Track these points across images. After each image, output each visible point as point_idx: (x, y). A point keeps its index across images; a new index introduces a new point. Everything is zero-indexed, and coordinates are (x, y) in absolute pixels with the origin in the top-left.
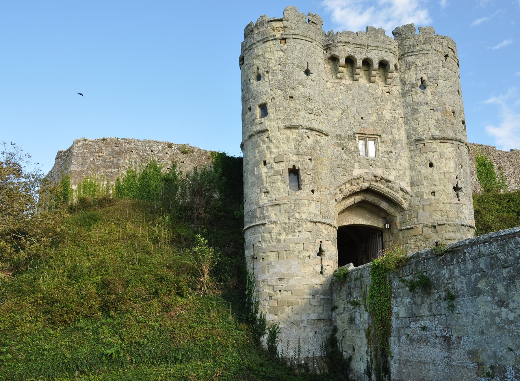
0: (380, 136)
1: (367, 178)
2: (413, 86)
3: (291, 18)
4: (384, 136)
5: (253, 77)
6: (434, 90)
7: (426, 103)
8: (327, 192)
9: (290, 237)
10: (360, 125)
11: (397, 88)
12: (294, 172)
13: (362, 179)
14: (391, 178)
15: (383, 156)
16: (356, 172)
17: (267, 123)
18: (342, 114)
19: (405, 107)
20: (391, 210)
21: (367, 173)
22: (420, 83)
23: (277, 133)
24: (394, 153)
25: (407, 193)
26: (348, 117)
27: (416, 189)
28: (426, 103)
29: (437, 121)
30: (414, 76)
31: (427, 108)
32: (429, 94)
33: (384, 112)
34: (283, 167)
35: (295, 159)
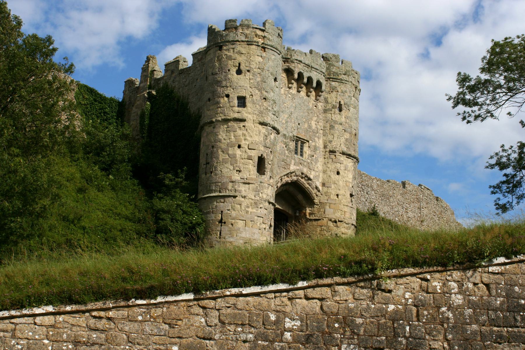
0: (308, 141)
1: (297, 174)
2: (334, 107)
7: (341, 124)
9: (254, 210)
12: (261, 161)
13: (294, 174)
14: (312, 177)
16: (293, 168)
17: (244, 113)
18: (288, 118)
19: (325, 122)
21: (298, 169)
23: (252, 125)
24: (314, 157)
25: (319, 191)
27: (325, 189)
29: (346, 140)
30: (335, 99)
31: (341, 128)
32: (343, 117)
34: (255, 155)
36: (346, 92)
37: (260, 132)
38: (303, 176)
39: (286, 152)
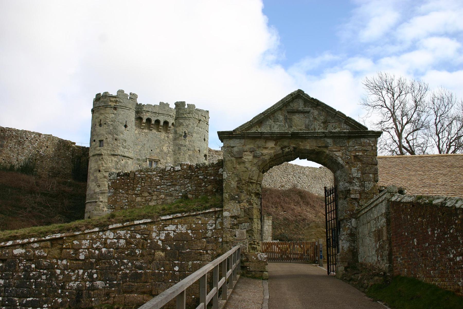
2: (181, 136)
3: (121, 96)
4: (162, 160)
5: (98, 124)
6: (190, 139)
7: (185, 146)
11: (172, 135)
22: (183, 135)
26: (144, 150)
28: (185, 146)
29: (189, 155)
33: (164, 148)
36: (189, 124)
37: (112, 160)
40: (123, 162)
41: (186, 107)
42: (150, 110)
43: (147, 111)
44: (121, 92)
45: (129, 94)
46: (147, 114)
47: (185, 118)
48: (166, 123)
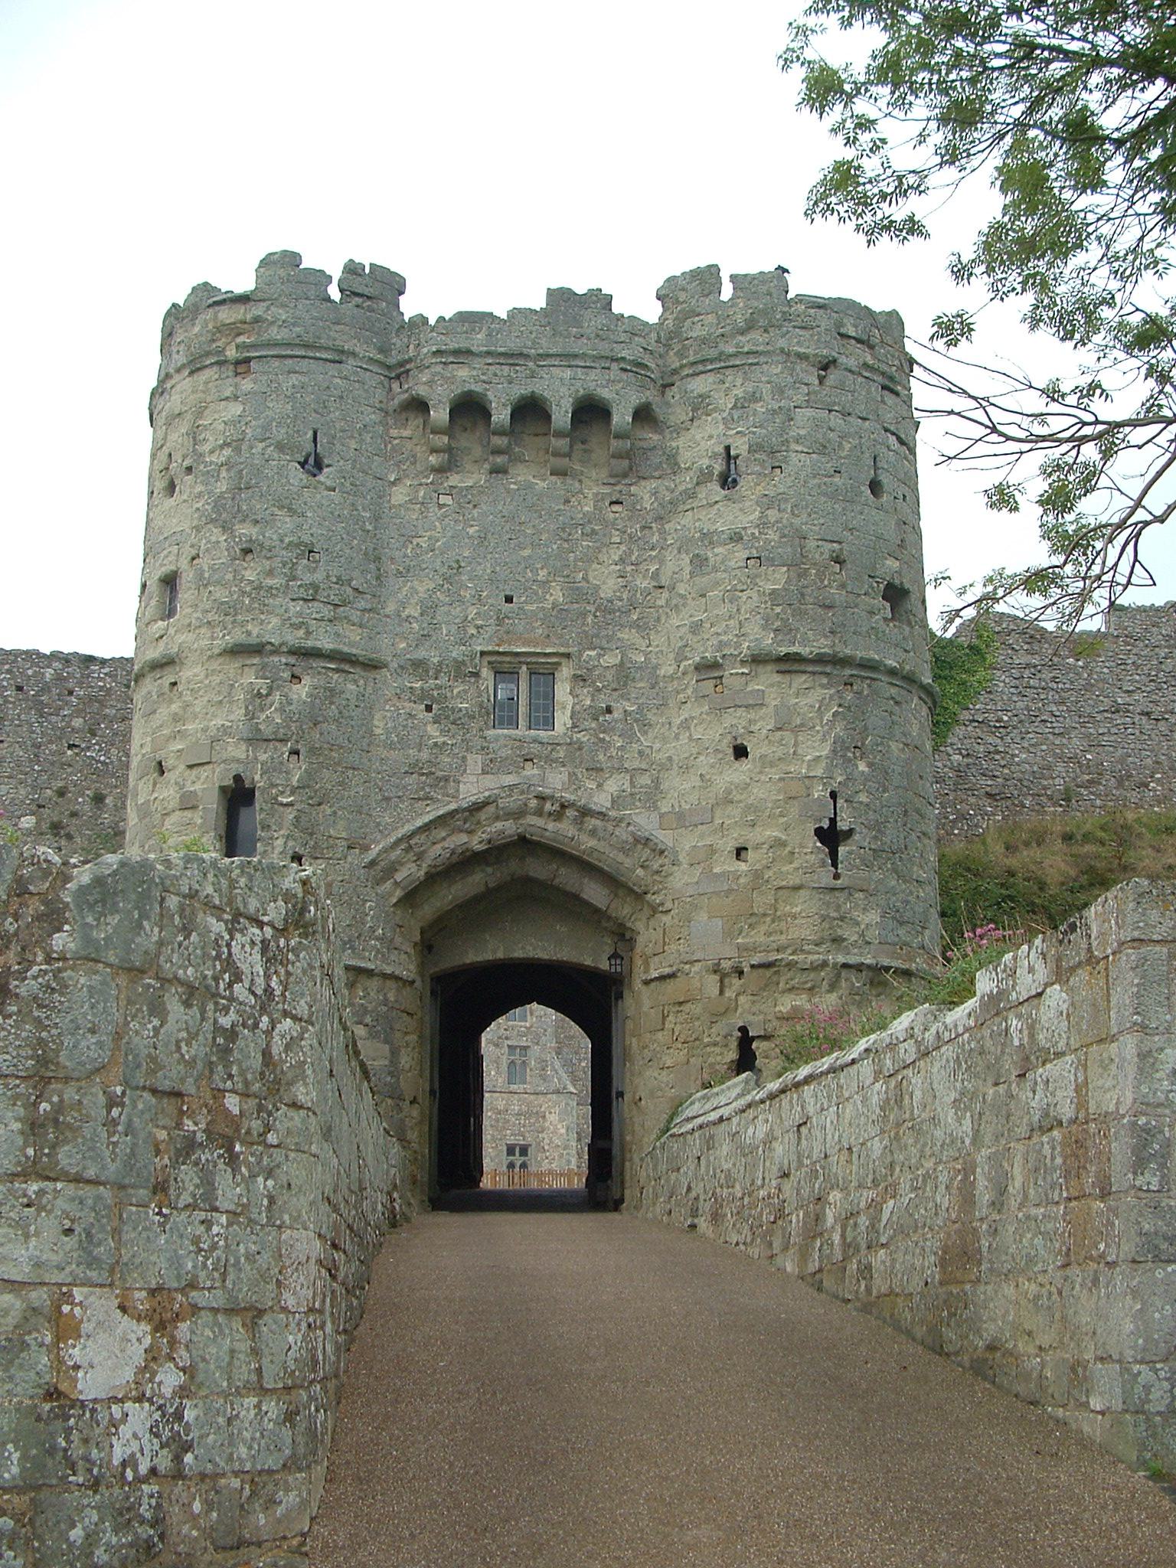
2: (704, 477)
7: (736, 538)
8: (354, 858)
10: (500, 621)
11: (653, 484)
13: (491, 809)
14: (601, 801)
15: (574, 726)
16: (472, 788)
20: (623, 910)
22: (718, 467)
34: (207, 785)
35: (244, 756)
36: (754, 397)
38: (548, 806)
39: (432, 730)
40: (301, 691)
41: (727, 292)
42: (478, 341)
43: (457, 352)
44: (282, 266)
45: (336, 272)
46: (463, 373)
47: (722, 364)
48: (591, 412)
